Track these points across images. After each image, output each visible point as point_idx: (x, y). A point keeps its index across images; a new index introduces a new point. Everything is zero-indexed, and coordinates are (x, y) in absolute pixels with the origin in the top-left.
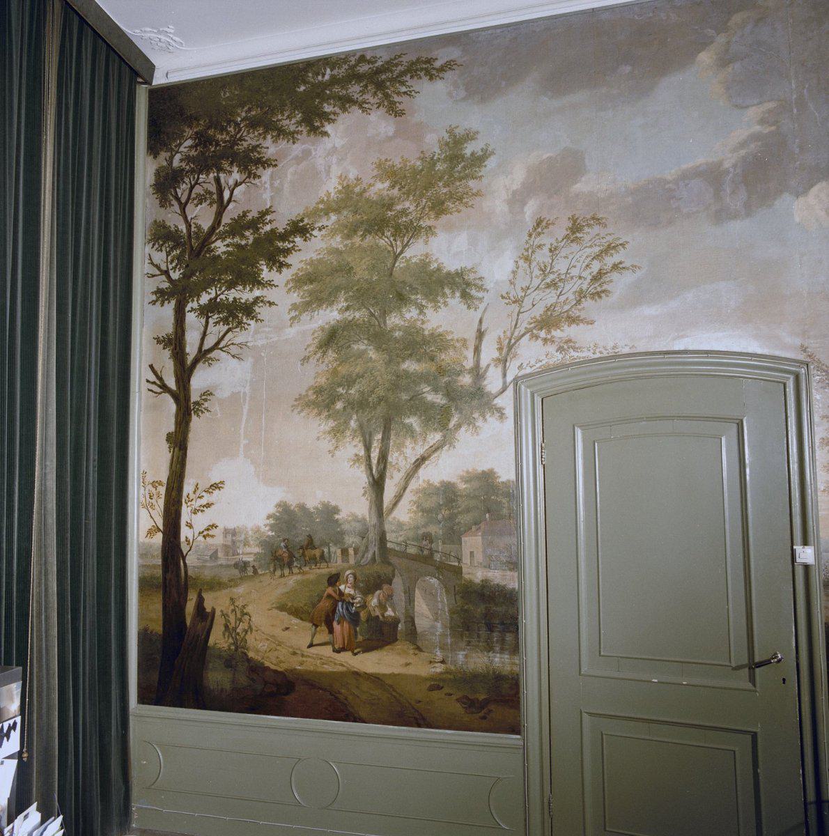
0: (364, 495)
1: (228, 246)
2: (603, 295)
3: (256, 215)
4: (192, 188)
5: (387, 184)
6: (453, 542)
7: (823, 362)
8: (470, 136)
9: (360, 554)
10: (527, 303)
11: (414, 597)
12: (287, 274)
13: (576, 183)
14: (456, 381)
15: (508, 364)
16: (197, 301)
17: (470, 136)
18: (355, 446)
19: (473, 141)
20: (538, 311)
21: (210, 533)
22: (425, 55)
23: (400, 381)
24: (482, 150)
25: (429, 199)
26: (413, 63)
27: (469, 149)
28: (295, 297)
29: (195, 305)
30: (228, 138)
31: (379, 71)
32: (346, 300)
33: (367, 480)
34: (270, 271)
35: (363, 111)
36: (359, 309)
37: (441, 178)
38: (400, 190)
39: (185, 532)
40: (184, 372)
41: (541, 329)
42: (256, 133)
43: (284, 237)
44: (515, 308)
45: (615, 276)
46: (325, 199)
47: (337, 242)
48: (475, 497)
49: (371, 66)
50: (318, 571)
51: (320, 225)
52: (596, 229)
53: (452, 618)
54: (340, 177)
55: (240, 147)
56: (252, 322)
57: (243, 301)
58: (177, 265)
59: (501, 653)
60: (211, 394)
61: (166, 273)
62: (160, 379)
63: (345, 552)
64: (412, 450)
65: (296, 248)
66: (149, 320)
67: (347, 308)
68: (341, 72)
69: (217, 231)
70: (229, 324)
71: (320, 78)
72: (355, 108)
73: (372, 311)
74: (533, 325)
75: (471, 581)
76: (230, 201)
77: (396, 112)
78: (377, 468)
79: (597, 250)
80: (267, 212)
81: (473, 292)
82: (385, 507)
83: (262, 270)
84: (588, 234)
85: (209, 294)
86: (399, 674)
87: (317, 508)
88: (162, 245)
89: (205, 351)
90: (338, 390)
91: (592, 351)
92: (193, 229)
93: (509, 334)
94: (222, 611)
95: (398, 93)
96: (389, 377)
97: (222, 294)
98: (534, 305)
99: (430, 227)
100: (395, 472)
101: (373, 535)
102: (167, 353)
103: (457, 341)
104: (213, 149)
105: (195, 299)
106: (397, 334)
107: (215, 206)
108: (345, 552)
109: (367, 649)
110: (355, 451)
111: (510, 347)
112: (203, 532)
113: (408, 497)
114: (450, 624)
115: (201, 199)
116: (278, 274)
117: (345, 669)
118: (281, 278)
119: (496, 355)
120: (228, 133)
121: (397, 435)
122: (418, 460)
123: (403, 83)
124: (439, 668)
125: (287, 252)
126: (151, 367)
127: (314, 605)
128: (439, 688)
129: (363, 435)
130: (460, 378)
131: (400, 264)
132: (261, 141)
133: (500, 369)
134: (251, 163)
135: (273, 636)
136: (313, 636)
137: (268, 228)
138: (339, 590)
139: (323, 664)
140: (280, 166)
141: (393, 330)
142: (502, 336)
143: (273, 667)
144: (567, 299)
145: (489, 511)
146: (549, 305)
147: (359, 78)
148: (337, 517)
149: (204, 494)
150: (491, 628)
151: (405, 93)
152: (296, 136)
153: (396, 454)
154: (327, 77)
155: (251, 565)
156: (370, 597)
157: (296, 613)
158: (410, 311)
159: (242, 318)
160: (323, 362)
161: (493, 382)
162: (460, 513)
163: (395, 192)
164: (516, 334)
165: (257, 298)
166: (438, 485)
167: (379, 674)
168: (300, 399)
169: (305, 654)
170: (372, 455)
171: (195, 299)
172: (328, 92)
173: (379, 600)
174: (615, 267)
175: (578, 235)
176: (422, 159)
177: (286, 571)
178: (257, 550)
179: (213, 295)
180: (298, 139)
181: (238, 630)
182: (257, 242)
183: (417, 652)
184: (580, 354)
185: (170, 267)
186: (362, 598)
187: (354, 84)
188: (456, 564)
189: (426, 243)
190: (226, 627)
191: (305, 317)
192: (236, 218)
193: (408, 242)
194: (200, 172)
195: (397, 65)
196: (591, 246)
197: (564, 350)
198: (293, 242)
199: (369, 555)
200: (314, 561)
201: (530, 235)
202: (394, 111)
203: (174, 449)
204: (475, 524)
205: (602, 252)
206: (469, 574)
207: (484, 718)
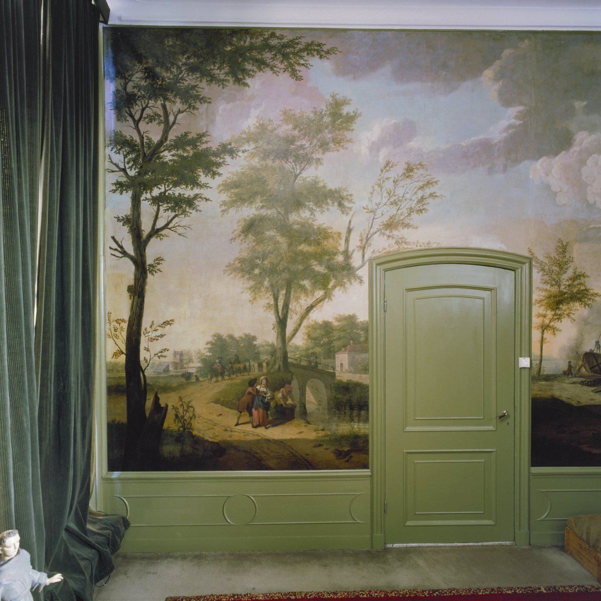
0: (273, 329)
1: (173, 155)
2: (423, 211)
3: (195, 136)
4: (143, 110)
5: (291, 126)
6: (330, 358)
8: (345, 102)
9: (270, 367)
10: (379, 212)
11: (305, 391)
12: (218, 180)
13: (411, 141)
14: (333, 259)
15: (366, 250)
16: (150, 193)
17: (345, 102)
18: (268, 298)
19: (348, 105)
20: (386, 219)
21: (163, 354)
22: (317, 41)
23: (297, 257)
24: (354, 112)
25: (319, 141)
26: (308, 45)
27: (345, 110)
28: (225, 197)
29: (148, 196)
30: (172, 77)
31: (285, 46)
32: (261, 202)
33: (275, 320)
34: (206, 177)
35: (274, 73)
37: (327, 127)
38: (299, 132)
39: (143, 354)
40: (140, 242)
41: (386, 230)
42: (194, 77)
43: (216, 155)
45: (431, 200)
46: (247, 131)
47: (256, 162)
49: (279, 41)
50: (242, 377)
51: (243, 149)
52: (421, 171)
53: (329, 403)
54: (258, 117)
55: (182, 85)
56: (194, 212)
57: (186, 196)
58: (133, 166)
59: (358, 423)
60: (163, 260)
61: (124, 170)
62: (121, 247)
64: (305, 301)
65: (226, 163)
66: (113, 205)
67: (262, 207)
68: (258, 41)
69: (165, 144)
70: (176, 212)
71: (242, 43)
73: (280, 210)
74: (382, 227)
76: (174, 123)
77: (297, 77)
78: (282, 313)
79: (421, 184)
80: (203, 135)
81: (346, 204)
82: (287, 336)
83: (200, 176)
84: (417, 173)
85: (160, 189)
86: (295, 439)
87: (241, 338)
88: (120, 149)
89: (157, 229)
90: (255, 261)
92: (145, 141)
94: (173, 406)
95: (299, 64)
96: (290, 254)
97: (170, 189)
98: (383, 215)
99: (319, 159)
100: (294, 315)
101: (279, 354)
102: (126, 229)
104: (160, 83)
105: (149, 192)
106: (295, 227)
107: (162, 125)
108: (260, 365)
109: (274, 425)
110: (267, 301)
111: (367, 239)
112: (157, 354)
115: (151, 119)
116: (212, 179)
117: (260, 438)
118: (215, 183)
119: (359, 244)
120: (172, 72)
121: (295, 291)
122: (308, 307)
123: (302, 57)
124: (321, 434)
125: (219, 165)
126: (113, 238)
128: (320, 445)
129: (273, 291)
130: (336, 257)
131: (299, 181)
132: (198, 83)
133: (361, 252)
134: (191, 98)
135: (211, 420)
136: (239, 419)
137: (204, 146)
138: (256, 389)
139: (245, 435)
140: (213, 104)
141: (293, 223)
143: (210, 440)
145: (352, 339)
146: (391, 216)
147: (271, 48)
148: (255, 343)
149: (159, 328)
150: (352, 408)
151: (303, 64)
152: (224, 83)
153: (295, 303)
154: (247, 44)
156: (276, 393)
157: (225, 404)
158: (305, 212)
159: (186, 208)
160: (245, 242)
161: (356, 260)
162: (335, 340)
163: (296, 133)
164: (371, 231)
165: (197, 195)
166: (321, 323)
167: (282, 439)
168: (229, 266)
169: (233, 430)
170: (279, 304)
171: (149, 192)
172: (248, 54)
173: (283, 394)
174: (431, 195)
175: (411, 174)
176: (315, 113)
177: (220, 378)
178: (199, 365)
179: (163, 190)
180: (226, 86)
181: (185, 418)
182: (195, 155)
183: (307, 424)
184: (409, 247)
185: (127, 166)
188: (332, 371)
190: (177, 416)
191: (232, 211)
192: (180, 136)
194: (150, 98)
195: (297, 44)
196: (418, 181)
197: (400, 243)
198: (223, 158)
200: (239, 371)
201: (382, 171)
202: (294, 75)
203: (134, 297)
204: (344, 347)
207: (348, 461)
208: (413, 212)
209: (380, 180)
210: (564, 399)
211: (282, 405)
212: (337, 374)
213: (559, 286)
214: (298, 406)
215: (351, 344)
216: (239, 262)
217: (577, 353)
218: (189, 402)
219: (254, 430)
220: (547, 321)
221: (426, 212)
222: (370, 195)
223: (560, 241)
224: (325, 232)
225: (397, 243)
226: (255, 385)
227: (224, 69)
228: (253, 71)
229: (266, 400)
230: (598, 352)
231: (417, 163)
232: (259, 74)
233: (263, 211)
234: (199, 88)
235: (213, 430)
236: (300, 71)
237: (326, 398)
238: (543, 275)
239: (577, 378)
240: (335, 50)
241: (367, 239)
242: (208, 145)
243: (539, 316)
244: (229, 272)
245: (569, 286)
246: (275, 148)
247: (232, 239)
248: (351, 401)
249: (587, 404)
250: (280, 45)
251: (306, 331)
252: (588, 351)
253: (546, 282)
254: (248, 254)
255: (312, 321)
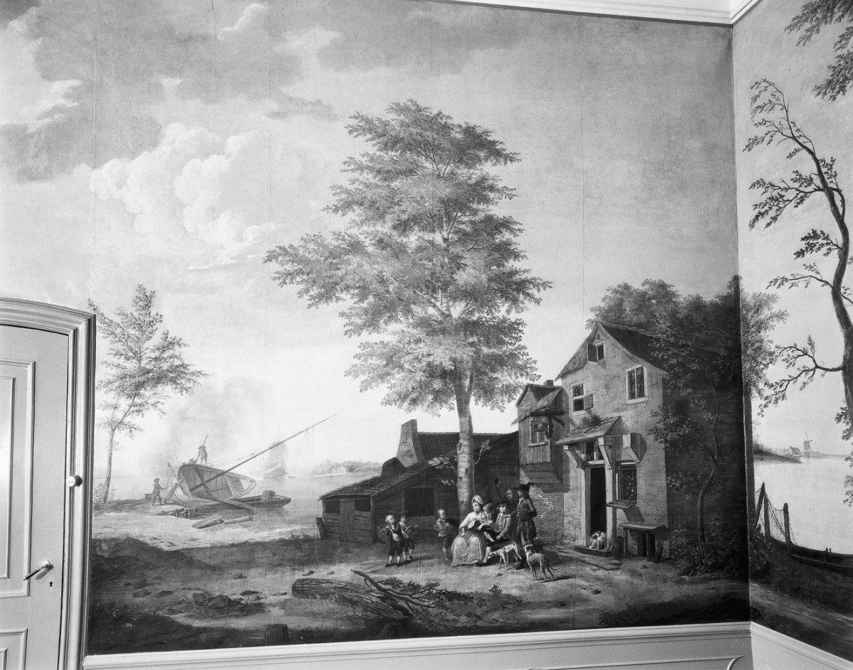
7: (105, 316)
210: (148, 541)
213: (140, 360)
217: (169, 465)
220: (119, 415)
223: (141, 288)
230: (204, 463)
238: (112, 342)
239: (169, 506)
243: (108, 406)
245: (156, 359)
249: (186, 546)
252: (187, 462)
253: (118, 354)
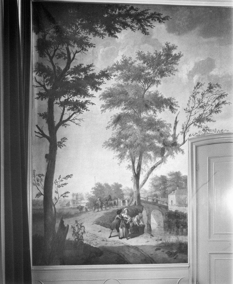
1: (73, 78)
2: (219, 112)
3: (86, 66)
4: (55, 50)
5: (142, 61)
6: (165, 197)
8: (174, 48)
9: (130, 202)
10: (193, 112)
12: (100, 92)
14: (167, 139)
15: (186, 134)
16: (59, 100)
17: (174, 48)
18: (128, 162)
19: (175, 50)
20: (197, 116)
21: (66, 195)
22: (158, 12)
24: (179, 53)
25: (158, 70)
27: (174, 52)
28: (103, 102)
29: (58, 101)
30: (72, 31)
31: (139, 14)
32: (125, 105)
33: (133, 175)
34: (92, 90)
35: (132, 30)
36: (130, 109)
37: (163, 62)
38: (147, 64)
39: (54, 195)
40: (53, 129)
41: (198, 122)
42: (86, 31)
43: (99, 77)
44: (189, 114)
45: (223, 105)
46: (116, 64)
47: (121, 82)
48: (173, 181)
49: (136, 12)
50: (113, 209)
52: (218, 88)
53: (164, 224)
55: (78, 36)
56: (85, 111)
57: (80, 102)
58: (49, 83)
60: (66, 139)
61: (44, 86)
62: (42, 131)
63: (124, 202)
64: (151, 164)
65: (104, 82)
66: (37, 105)
67: (125, 109)
68: (123, 12)
69: (68, 71)
70: (74, 111)
71: (114, 12)
72: (129, 29)
73: (135, 110)
74: (195, 121)
75: (171, 211)
76: (73, 58)
78: (137, 170)
79: (217, 96)
80: (91, 66)
81: (174, 107)
82: (140, 185)
83: (89, 90)
84: (215, 90)
85: (65, 97)
87: (113, 185)
88: (41, 74)
89: (63, 121)
91: (214, 131)
92: (56, 69)
93: (186, 123)
94: (72, 226)
95: (147, 25)
96: (142, 136)
97: (71, 98)
98: (195, 114)
99: (159, 81)
100: (144, 172)
101: (135, 195)
102: (45, 121)
103: (168, 124)
104: (65, 35)
105: (58, 99)
106: (145, 120)
107: (66, 60)
108: (124, 202)
109: (132, 237)
110: (129, 163)
111: (187, 128)
112: (63, 195)
113: (149, 181)
114: (164, 226)
115: (60, 56)
116: (96, 92)
117: (124, 245)
118: (97, 94)
119: (182, 130)
120: (72, 29)
121: (145, 158)
122: (152, 167)
123: (149, 22)
124: (160, 242)
125: (100, 83)
126: (37, 126)
127: (111, 222)
128: (159, 249)
129: (132, 157)
130: (169, 138)
131: (147, 94)
132: (88, 35)
133: (183, 135)
134: (83, 44)
135: (94, 234)
136: (111, 233)
137: (91, 72)
139: (115, 243)
140: (96, 48)
141: (143, 118)
142: (184, 124)
143: (94, 246)
144: (207, 112)
145: (178, 186)
146: (200, 114)
147: (131, 16)
148: (121, 188)
149: (63, 179)
150: (178, 227)
151: (149, 26)
153: (144, 165)
154: (117, 13)
155: (85, 207)
156: (133, 218)
157: (104, 225)
158: (150, 112)
159: (80, 109)
161: (180, 140)
162: (168, 187)
163: (145, 65)
164: (189, 123)
168: (106, 143)
169: (108, 240)
170: (135, 165)
171: (58, 99)
172: (117, 19)
173: (137, 219)
174: (223, 102)
175: (212, 90)
176: (156, 54)
177: (100, 209)
178: (87, 201)
179: (67, 98)
180: (104, 37)
181: (79, 233)
183: (151, 237)
184: (210, 132)
185: (46, 84)
186: (131, 219)
187: (129, 18)
188: (166, 205)
189: (157, 86)
190: (74, 232)
191: (108, 110)
192: (77, 66)
193: (150, 85)
194: (59, 44)
195: (146, 13)
196: (216, 94)
197: (205, 130)
198: (103, 80)
199: (134, 203)
200: (111, 205)
201: (195, 88)
202: (144, 31)
203: (49, 161)
204: (173, 191)
205: (219, 97)
206: (171, 208)
207: (175, 258)
208: (213, 112)
209: (194, 93)
211: (137, 225)
212: (169, 207)
214: (146, 226)
215: (178, 189)
216: (112, 141)
218: (81, 224)
219: (120, 240)
221: (220, 112)
222: (188, 102)
224: (162, 123)
225: (204, 130)
226: (121, 213)
227: (103, 27)
228: (120, 29)
229: (127, 222)
231: (215, 84)
232: (123, 31)
233: (125, 110)
234: (88, 38)
235: (96, 240)
236: (147, 29)
237: (163, 221)
240: (168, 17)
241: (187, 128)
242: (94, 72)
244: (105, 147)
246: (133, 74)
247: (107, 127)
248: (176, 221)
250: (136, 14)
251: (151, 181)
254: (117, 136)
255: (155, 175)
